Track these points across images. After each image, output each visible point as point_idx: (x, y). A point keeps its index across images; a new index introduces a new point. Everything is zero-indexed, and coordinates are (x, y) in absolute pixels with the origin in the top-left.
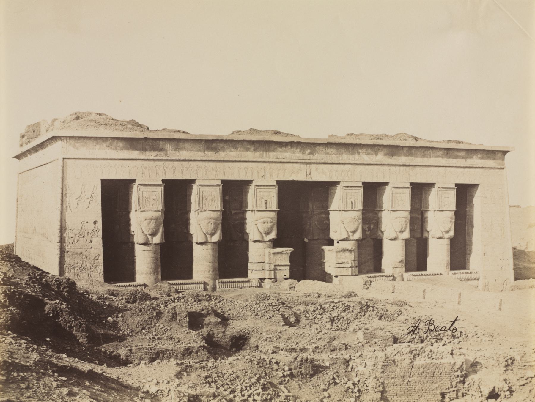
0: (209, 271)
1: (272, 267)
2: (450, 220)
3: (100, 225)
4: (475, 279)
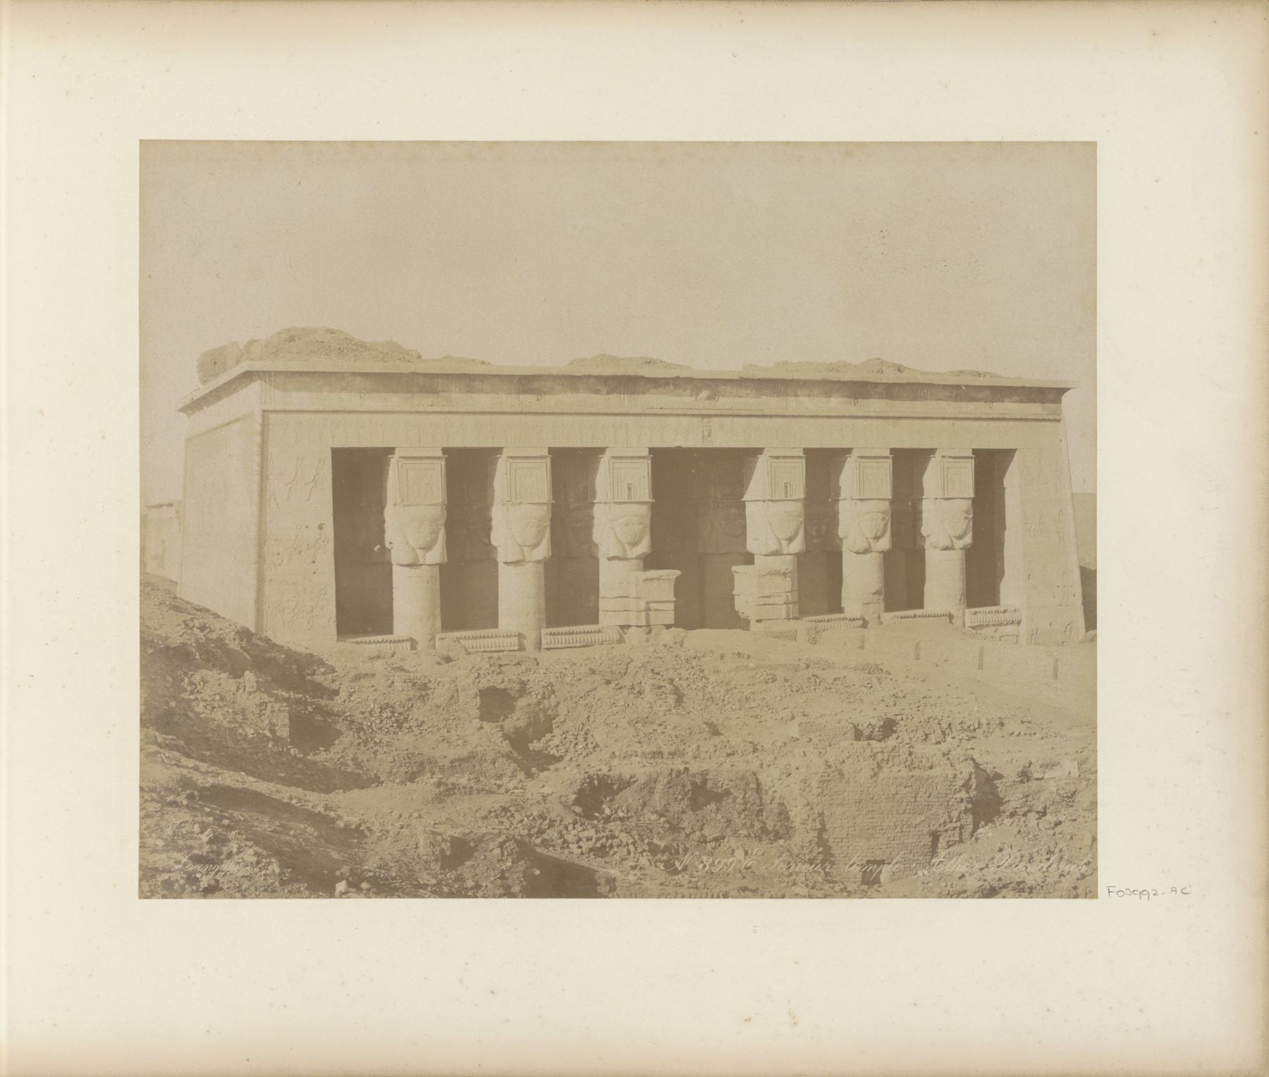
1: (643, 605)
2: (965, 515)
3: (329, 530)
4: (1012, 623)
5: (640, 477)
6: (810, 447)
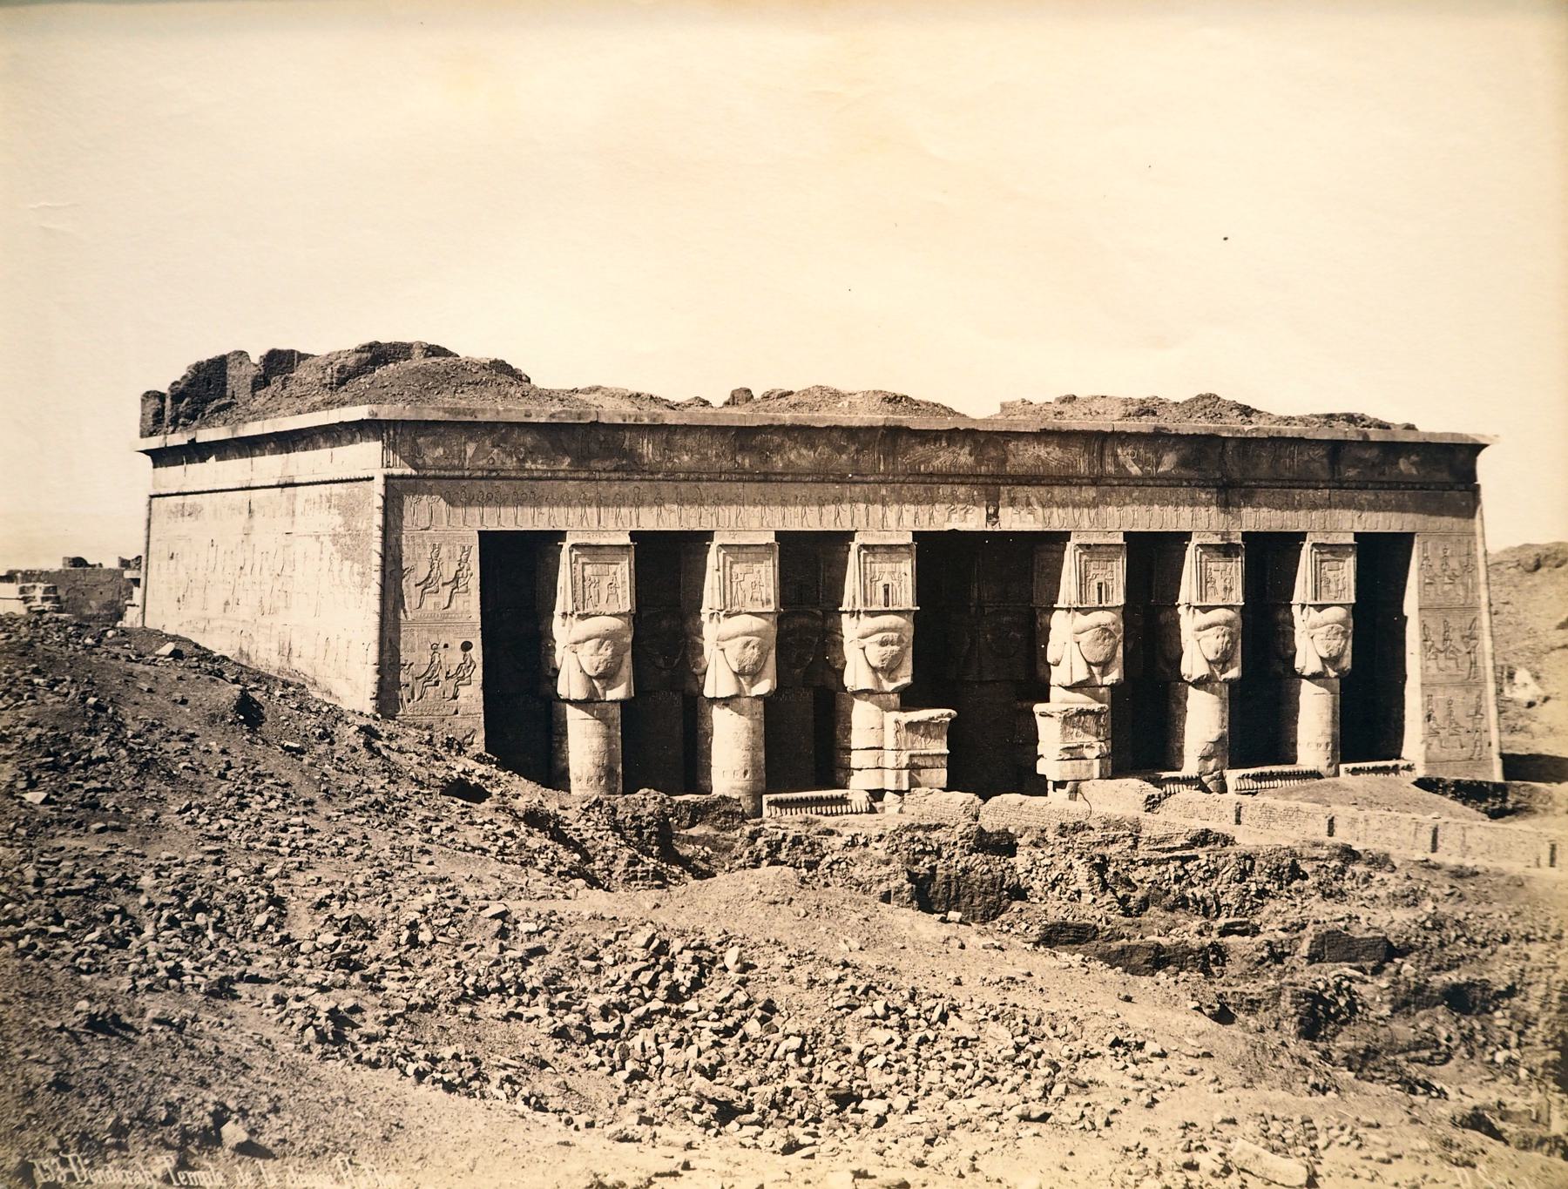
0: (745, 773)
1: (905, 760)
3: (476, 653)
5: (901, 578)
6: (1134, 530)
